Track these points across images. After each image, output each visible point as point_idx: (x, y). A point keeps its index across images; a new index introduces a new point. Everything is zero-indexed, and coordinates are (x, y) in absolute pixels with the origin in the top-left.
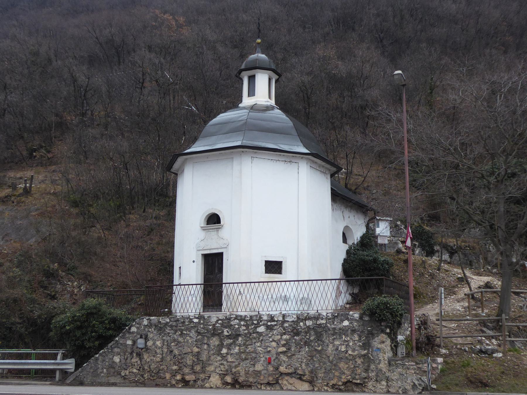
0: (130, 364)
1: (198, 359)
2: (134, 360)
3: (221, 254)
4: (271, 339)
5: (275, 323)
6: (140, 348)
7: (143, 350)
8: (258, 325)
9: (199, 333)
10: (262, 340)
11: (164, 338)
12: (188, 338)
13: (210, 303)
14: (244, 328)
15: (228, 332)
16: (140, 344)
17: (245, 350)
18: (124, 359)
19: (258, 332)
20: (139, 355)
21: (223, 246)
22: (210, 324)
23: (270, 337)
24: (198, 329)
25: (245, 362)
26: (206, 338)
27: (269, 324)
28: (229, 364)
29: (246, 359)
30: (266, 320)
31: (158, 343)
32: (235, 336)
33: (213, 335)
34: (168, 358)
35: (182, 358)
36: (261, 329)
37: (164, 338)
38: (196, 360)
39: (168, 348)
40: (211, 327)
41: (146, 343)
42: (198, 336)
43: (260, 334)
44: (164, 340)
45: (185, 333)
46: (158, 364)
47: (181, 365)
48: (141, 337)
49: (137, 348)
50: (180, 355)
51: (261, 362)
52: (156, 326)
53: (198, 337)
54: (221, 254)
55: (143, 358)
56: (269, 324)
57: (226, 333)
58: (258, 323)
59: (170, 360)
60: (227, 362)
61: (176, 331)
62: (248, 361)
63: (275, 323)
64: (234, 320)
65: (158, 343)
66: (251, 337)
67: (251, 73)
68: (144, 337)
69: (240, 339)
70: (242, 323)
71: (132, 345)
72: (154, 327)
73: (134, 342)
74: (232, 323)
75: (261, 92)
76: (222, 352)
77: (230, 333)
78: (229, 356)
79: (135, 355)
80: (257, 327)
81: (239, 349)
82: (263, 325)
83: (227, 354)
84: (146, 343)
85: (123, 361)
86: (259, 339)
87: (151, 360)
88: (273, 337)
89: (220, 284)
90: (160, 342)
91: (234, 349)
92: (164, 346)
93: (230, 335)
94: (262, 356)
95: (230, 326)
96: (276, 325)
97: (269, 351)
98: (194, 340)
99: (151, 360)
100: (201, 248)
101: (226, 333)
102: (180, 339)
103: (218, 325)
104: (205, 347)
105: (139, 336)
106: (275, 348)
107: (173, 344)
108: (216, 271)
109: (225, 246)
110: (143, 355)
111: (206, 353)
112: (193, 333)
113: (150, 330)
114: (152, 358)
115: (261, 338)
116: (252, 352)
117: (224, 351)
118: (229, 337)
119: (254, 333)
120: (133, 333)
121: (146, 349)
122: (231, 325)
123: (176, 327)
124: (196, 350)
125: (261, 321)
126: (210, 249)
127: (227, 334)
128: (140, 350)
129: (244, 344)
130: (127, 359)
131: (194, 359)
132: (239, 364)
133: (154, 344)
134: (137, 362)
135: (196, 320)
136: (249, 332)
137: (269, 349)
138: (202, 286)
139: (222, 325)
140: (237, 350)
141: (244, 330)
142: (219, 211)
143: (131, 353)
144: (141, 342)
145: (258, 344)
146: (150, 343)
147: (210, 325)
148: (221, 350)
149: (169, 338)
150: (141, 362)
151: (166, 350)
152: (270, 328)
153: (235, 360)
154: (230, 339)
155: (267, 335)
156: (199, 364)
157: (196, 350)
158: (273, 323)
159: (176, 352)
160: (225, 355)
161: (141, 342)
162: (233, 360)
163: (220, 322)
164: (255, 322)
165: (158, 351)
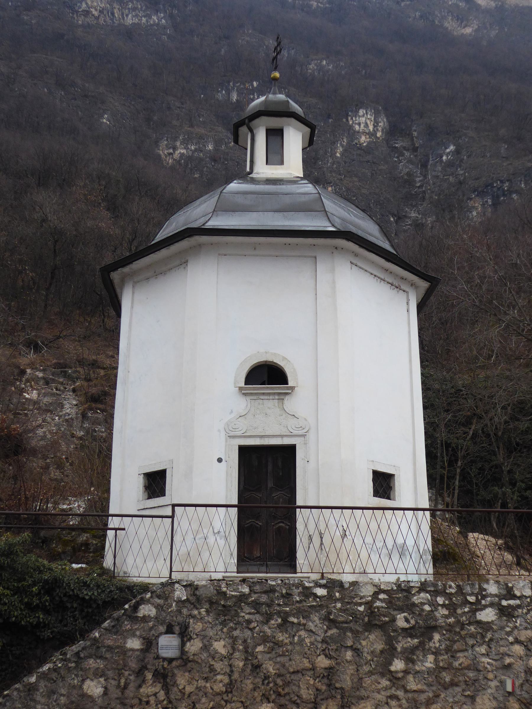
0: (136, 701)
1: (329, 685)
2: (147, 690)
3: (292, 449)
4: (511, 639)
5: (518, 602)
6: (164, 659)
7: (174, 663)
8: (477, 607)
9: (331, 621)
10: (491, 640)
11: (236, 633)
12: (302, 633)
13: (257, 553)
14: (446, 612)
15: (407, 620)
16: (167, 647)
17: (450, 664)
18: (118, 686)
19: (479, 622)
20: (163, 677)
21: (295, 432)
22: (357, 600)
23: (509, 634)
24: (330, 613)
25: (450, 690)
26: (349, 634)
27: (504, 603)
28: (410, 695)
29: (453, 684)
30: (496, 595)
31: (220, 647)
32: (425, 629)
33: (370, 627)
34: (248, 684)
35: (287, 684)
36: (488, 615)
37: (236, 633)
38: (324, 688)
39: (246, 659)
40: (361, 609)
41: (183, 644)
42: (329, 628)
43: (486, 626)
44: (234, 639)
45: (295, 620)
46: (218, 698)
47: (283, 701)
48: (169, 631)
49: (158, 657)
50: (279, 675)
51: (489, 691)
52: (211, 603)
53: (330, 633)
54: (292, 449)
55: (175, 684)
56: (504, 603)
57: (401, 623)
58: (478, 601)
59: (254, 689)
60: (406, 691)
61: (268, 618)
62: (458, 689)
63: (518, 602)
64: (419, 592)
65: (220, 647)
66: (463, 633)
67: (274, 122)
68: (177, 629)
69: (437, 637)
70: (440, 600)
71: (142, 650)
72: (207, 606)
73: (150, 644)
74: (416, 599)
75: (284, 163)
76: (393, 668)
77: (413, 622)
78: (410, 678)
79: (149, 676)
80: (481, 610)
81: (436, 660)
82: (492, 605)
83: (406, 672)
84: (183, 644)
85: (115, 693)
86: (483, 637)
87: (198, 688)
88: (516, 632)
89: (288, 510)
90: (222, 643)
91: (422, 661)
92: (237, 654)
93: (411, 628)
94: (491, 676)
95: (410, 607)
96: (519, 607)
97: (509, 666)
98: (319, 639)
99: (198, 688)
100: (239, 433)
101: (401, 623)
102: (281, 637)
103: (378, 604)
104: (349, 655)
105: (162, 629)
106: (521, 658)
107: (260, 649)
108: (270, 484)
109: (301, 432)
110: (174, 675)
111: (351, 670)
112: (315, 622)
113: (196, 612)
114: (201, 683)
115: (489, 635)
116: (468, 668)
117: (398, 665)
118: (408, 632)
119: (470, 624)
120: (145, 619)
121: (184, 660)
122: (414, 605)
123: (269, 606)
124: (323, 662)
125: (484, 597)
126: (262, 437)
127: (405, 625)
128: (166, 664)
129: (448, 650)
130: (126, 687)
131: (319, 685)
132: (438, 696)
133: (206, 648)
134: (155, 695)
135: (321, 592)
136: (458, 622)
137: (508, 661)
138: (234, 511)
139: (390, 602)
140: (429, 662)
141: (446, 617)
142: (284, 359)
143: (140, 673)
144: (168, 645)
145: (483, 650)
146: (194, 647)
147: (360, 604)
148: (390, 664)
149: (249, 633)
150: (167, 694)
151: (241, 664)
152: (505, 613)
153: (425, 687)
154: (412, 636)
155: (502, 628)
156: (333, 697)
157: (323, 662)
158: (512, 602)
159: (270, 668)
160: (400, 675)
161: (168, 645)
162: (420, 687)
163: (382, 596)
164: (472, 599)
165: (218, 666)
